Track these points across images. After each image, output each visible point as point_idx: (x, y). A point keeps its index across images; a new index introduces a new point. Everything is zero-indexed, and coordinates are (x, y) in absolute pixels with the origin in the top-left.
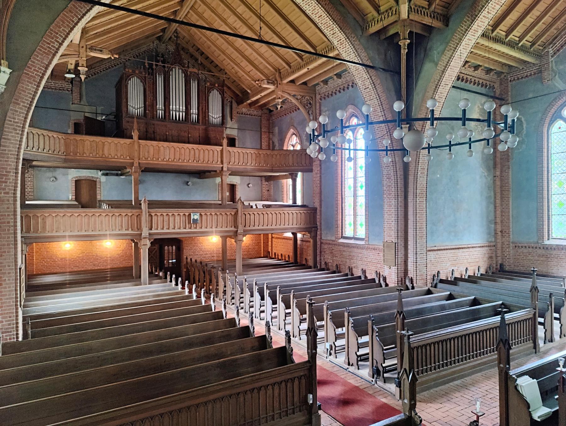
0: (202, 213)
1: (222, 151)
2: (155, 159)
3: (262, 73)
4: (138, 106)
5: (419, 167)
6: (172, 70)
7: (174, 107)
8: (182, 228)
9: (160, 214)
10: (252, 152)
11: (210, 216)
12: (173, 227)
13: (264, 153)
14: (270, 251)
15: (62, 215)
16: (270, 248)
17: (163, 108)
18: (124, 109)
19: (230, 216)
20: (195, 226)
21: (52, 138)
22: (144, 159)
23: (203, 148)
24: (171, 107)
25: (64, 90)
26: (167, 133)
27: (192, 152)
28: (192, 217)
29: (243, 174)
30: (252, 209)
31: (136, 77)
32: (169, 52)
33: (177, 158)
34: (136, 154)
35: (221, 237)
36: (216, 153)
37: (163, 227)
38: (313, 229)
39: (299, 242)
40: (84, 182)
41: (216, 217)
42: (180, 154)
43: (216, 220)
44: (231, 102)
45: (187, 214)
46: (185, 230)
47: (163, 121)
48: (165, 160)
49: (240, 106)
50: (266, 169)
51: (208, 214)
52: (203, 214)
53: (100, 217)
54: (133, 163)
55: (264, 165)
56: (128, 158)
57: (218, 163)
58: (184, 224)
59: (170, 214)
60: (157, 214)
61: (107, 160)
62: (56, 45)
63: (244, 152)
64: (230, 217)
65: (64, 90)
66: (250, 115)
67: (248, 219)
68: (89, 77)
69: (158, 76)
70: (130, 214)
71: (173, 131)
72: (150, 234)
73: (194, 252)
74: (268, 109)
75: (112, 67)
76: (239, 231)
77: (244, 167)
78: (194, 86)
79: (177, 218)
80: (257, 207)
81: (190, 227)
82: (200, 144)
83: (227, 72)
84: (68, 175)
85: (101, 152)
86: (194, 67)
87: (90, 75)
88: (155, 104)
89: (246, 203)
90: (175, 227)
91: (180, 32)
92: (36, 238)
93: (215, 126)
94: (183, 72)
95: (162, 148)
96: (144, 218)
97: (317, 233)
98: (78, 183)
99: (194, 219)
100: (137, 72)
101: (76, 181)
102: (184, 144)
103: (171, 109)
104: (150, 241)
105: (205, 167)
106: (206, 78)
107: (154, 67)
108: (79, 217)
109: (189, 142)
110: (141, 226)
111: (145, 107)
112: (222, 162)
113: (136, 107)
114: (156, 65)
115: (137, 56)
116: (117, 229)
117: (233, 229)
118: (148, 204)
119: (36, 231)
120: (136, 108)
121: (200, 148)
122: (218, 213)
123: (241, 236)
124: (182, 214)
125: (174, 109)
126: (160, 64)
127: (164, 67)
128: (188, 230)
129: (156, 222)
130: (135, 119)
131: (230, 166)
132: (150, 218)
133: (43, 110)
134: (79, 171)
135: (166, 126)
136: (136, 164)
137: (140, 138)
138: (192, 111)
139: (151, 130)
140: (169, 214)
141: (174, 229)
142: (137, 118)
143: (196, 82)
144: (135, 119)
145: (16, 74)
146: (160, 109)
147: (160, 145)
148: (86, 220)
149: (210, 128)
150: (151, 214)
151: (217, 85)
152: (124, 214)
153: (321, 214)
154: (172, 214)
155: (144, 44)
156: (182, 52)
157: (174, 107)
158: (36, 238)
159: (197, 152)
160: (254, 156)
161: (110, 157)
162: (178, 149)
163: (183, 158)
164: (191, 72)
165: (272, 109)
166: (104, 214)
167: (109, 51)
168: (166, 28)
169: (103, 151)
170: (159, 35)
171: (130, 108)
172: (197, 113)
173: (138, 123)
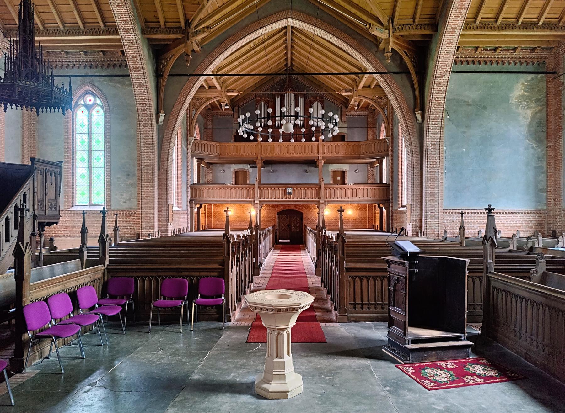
1: (318, 145)
3: (347, 84)
5: (429, 144)
11: (300, 190)
13: (353, 144)
15: (212, 188)
21: (212, 146)
27: (297, 147)
28: (287, 191)
33: (286, 152)
34: (259, 152)
41: (304, 191)
42: (288, 149)
43: (304, 193)
44: (341, 108)
45: (284, 189)
50: (354, 157)
52: (295, 189)
59: (273, 189)
62: (184, 99)
64: (315, 192)
70: (248, 188)
73: (311, 222)
74: (370, 109)
78: (301, 101)
79: (277, 191)
96: (257, 191)
98: (236, 173)
99: (288, 192)
101: (236, 172)
105: (305, 157)
108: (220, 190)
117: (317, 199)
119: (199, 197)
122: (306, 188)
123: (323, 205)
124: (280, 189)
128: (284, 199)
133: (218, 129)
136: (259, 158)
145: (167, 116)
151: (318, 98)
152: (245, 188)
153: (392, 190)
162: (286, 146)
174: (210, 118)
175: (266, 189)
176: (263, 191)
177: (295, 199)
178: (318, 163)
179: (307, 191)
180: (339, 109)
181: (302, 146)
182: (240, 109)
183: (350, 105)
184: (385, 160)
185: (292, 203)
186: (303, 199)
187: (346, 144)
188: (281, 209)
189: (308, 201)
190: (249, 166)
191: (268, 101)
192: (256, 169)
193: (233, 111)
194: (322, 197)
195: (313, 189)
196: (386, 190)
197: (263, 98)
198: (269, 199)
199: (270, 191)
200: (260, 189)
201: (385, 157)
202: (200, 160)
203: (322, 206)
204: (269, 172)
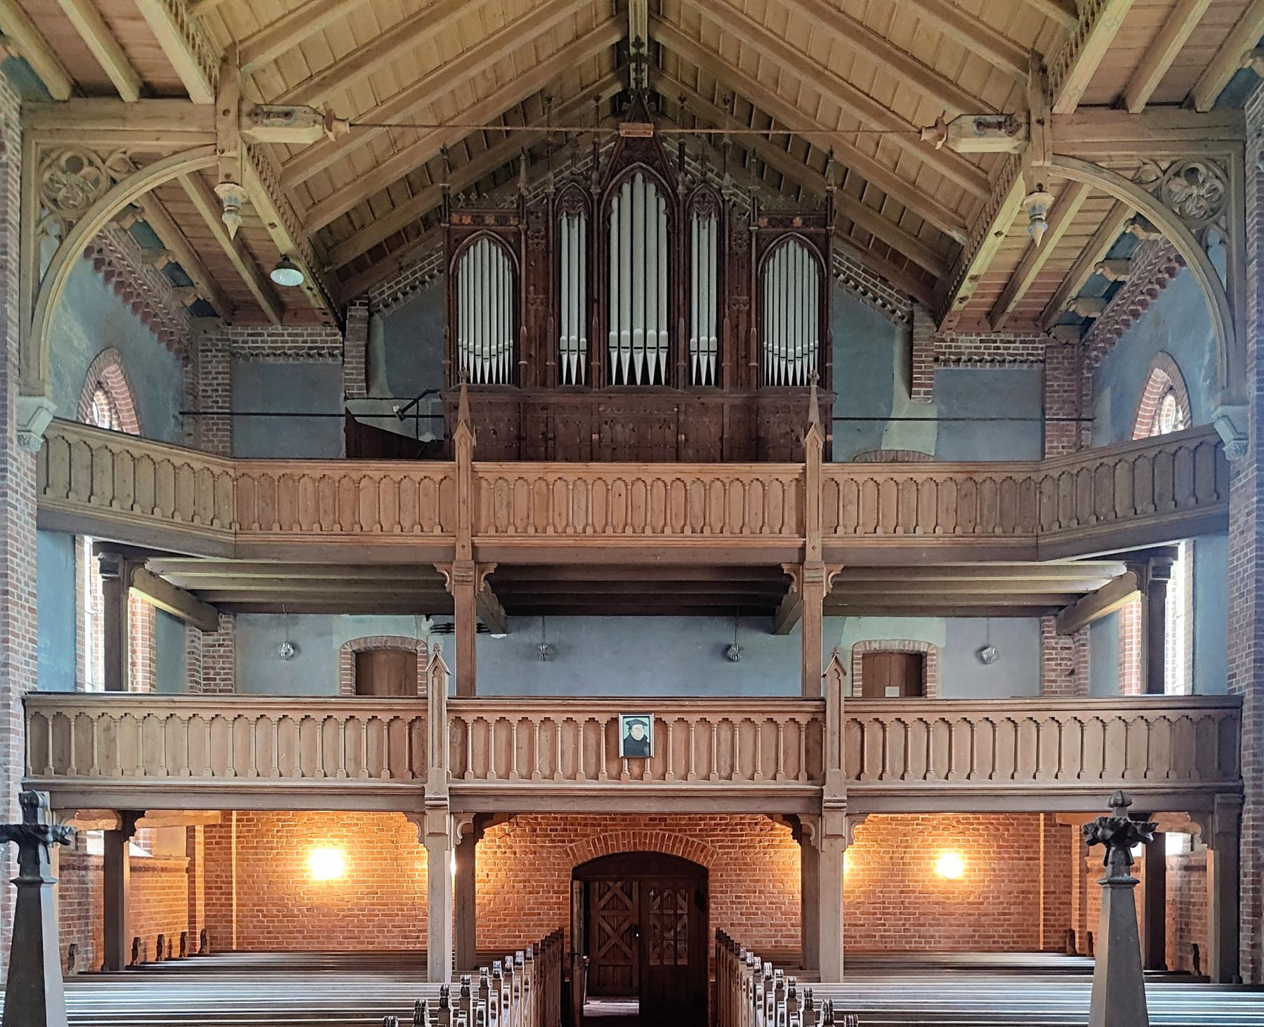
0: (665, 718)
1: (801, 482)
2: (531, 530)
11: (702, 730)
12: (547, 772)
13: (998, 478)
14: (1077, 929)
16: (1076, 915)
19: (792, 728)
20: (636, 770)
22: (492, 532)
25: (320, 355)
26: (595, 437)
27: (678, 494)
28: (623, 733)
33: (618, 517)
34: (465, 517)
37: (509, 769)
38: (1218, 798)
39: (1173, 877)
40: (383, 657)
41: (725, 733)
42: (630, 506)
43: (725, 747)
45: (603, 719)
47: (576, 391)
48: (570, 531)
50: (1006, 547)
52: (669, 719)
53: (283, 723)
54: (454, 547)
55: (998, 531)
56: (437, 530)
58: (593, 760)
59: (536, 719)
61: (362, 538)
64: (790, 739)
65: (320, 355)
67: (873, 746)
68: (396, 299)
70: (385, 717)
71: (618, 427)
81: (614, 773)
84: (331, 633)
85: (347, 519)
87: (400, 295)
90: (553, 771)
92: (83, 793)
93: (784, 385)
97: (1241, 814)
99: (629, 740)
103: (613, 343)
104: (458, 821)
110: (424, 764)
111: (516, 347)
112: (801, 530)
116: (341, 774)
117: (802, 784)
119: (86, 766)
121: (707, 479)
122: (736, 718)
128: (604, 784)
129: (480, 749)
131: (834, 543)
132: (459, 732)
134: (361, 621)
136: (464, 554)
137: (478, 456)
141: (551, 777)
148: (239, 737)
150: (463, 717)
158: (83, 793)
159: (696, 492)
160: (949, 493)
163: (638, 521)
165: (1083, 314)
166: (298, 716)
169: (355, 509)
171: (463, 355)
172: (714, 347)
174: (217, 365)
176: (475, 736)
177: (673, 783)
178: (802, 582)
179: (744, 736)
180: (899, 329)
181: (707, 489)
182: (377, 317)
183: (966, 289)
184: (1180, 571)
185: (654, 807)
186: (716, 784)
187: (960, 477)
188: (587, 851)
189: (746, 796)
191: (517, 235)
192: (452, 638)
193: (342, 328)
194: (832, 771)
195: (781, 719)
196: (1213, 728)
197: (490, 220)
199: (519, 736)
200: (459, 722)
201: (1182, 547)
202: (118, 559)
203: (834, 822)
204: (532, 653)
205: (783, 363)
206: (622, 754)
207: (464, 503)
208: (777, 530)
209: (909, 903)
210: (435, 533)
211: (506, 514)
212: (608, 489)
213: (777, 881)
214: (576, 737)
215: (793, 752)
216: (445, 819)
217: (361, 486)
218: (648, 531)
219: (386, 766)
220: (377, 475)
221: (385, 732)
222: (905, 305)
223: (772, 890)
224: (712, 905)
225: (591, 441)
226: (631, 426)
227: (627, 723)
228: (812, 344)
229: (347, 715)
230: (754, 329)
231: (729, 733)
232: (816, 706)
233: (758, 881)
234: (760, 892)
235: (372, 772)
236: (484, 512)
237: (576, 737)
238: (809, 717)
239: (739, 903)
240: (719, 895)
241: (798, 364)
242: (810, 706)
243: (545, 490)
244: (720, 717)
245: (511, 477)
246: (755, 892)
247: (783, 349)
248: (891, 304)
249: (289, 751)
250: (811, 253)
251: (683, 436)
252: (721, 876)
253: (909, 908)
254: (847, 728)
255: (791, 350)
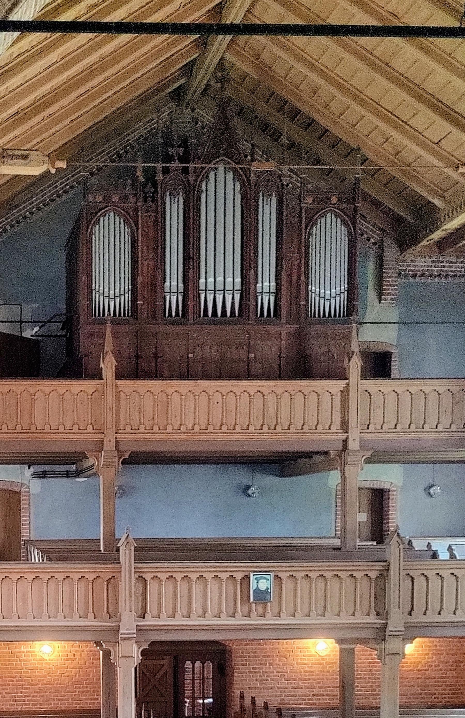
4: (117, 290)
6: (207, 177)
7: (211, 280)
8: (223, 616)
9: (167, 575)
10: (441, 390)
12: (200, 612)
17: (181, 290)
18: (84, 302)
20: (261, 610)
23: (290, 389)
24: (202, 280)
26: (191, 355)
28: (253, 585)
29: (412, 457)
30: (434, 562)
31: (112, 214)
32: (203, 128)
33: (216, 419)
34: (110, 419)
35: (340, 641)
36: (326, 398)
41: (321, 583)
43: (321, 593)
45: (239, 576)
46: (232, 621)
47: (179, 324)
48: (183, 428)
49: (410, 251)
51: (299, 575)
52: (283, 575)
56: (90, 429)
57: (333, 429)
58: (232, 604)
59: (194, 576)
60: (159, 575)
63: (413, 389)
66: (439, 276)
69: (168, 201)
70: (91, 577)
71: (207, 348)
72: (140, 630)
75: (59, 196)
76: (390, 628)
77: (412, 435)
79: (212, 587)
80: (453, 556)
81: (246, 612)
82: (280, 377)
83: (371, 156)
86: (268, 155)
88: (160, 278)
89: (419, 545)
90: (205, 612)
91: (233, 65)
94: (237, 176)
95: (176, 397)
99: (257, 591)
100: (115, 198)
102: (235, 382)
106: (304, 183)
107: (160, 177)
109: (249, 376)
113: (112, 292)
114: (166, 171)
115: (119, 156)
116: (60, 616)
118: (136, 550)
120: (112, 296)
121: (279, 391)
122: (328, 575)
124: (224, 576)
125: (210, 287)
126: (176, 164)
127: (185, 171)
128: (239, 621)
130: (108, 324)
132: (140, 586)
135: (187, 336)
136: (109, 446)
137: (119, 376)
138: (259, 285)
139: (148, 351)
140: (190, 575)
142: (112, 322)
143: (274, 200)
144: (108, 324)
146: (174, 289)
147: (170, 390)
149: (313, 330)
152: (76, 577)
154: (198, 575)
155: (138, 118)
156: (236, 122)
157: (211, 280)
161: (47, 430)
162: (218, 397)
164: (259, 174)
167: (49, 156)
168: (193, 62)
170: (176, 85)
172: (273, 290)
173: (115, 335)
175: (163, 576)
176: (152, 587)
179: (334, 585)
190: (28, 472)
195: (359, 575)
198: (179, 621)
199: (182, 587)
200: (142, 579)
205: (322, 301)
206: (252, 600)
207: (110, 409)
208: (327, 427)
209: (376, 671)
210: (88, 431)
211: (137, 417)
212: (209, 399)
213: (281, 656)
214: (220, 588)
215: (366, 596)
216: (133, 645)
217: (36, 397)
218: (238, 429)
219: (91, 610)
220: (47, 390)
221: (90, 587)
222: (377, 235)
223: (278, 663)
224: (236, 674)
225: (188, 357)
226: (216, 347)
227: (256, 579)
228: (342, 288)
229: (62, 576)
230: (303, 278)
231: (323, 584)
232: (383, 566)
233: (268, 656)
234: (270, 664)
235: (81, 614)
236: (122, 415)
237: (220, 588)
238: (377, 573)
239: (255, 672)
240: (241, 667)
241: (333, 301)
242: (379, 566)
243: (165, 399)
244: (318, 574)
245: (142, 390)
246: (266, 664)
247: (322, 291)
248: (367, 234)
249: (25, 601)
250: (344, 222)
251: (253, 355)
252: (242, 653)
253: (375, 674)
254: (404, 580)
255: (328, 292)
